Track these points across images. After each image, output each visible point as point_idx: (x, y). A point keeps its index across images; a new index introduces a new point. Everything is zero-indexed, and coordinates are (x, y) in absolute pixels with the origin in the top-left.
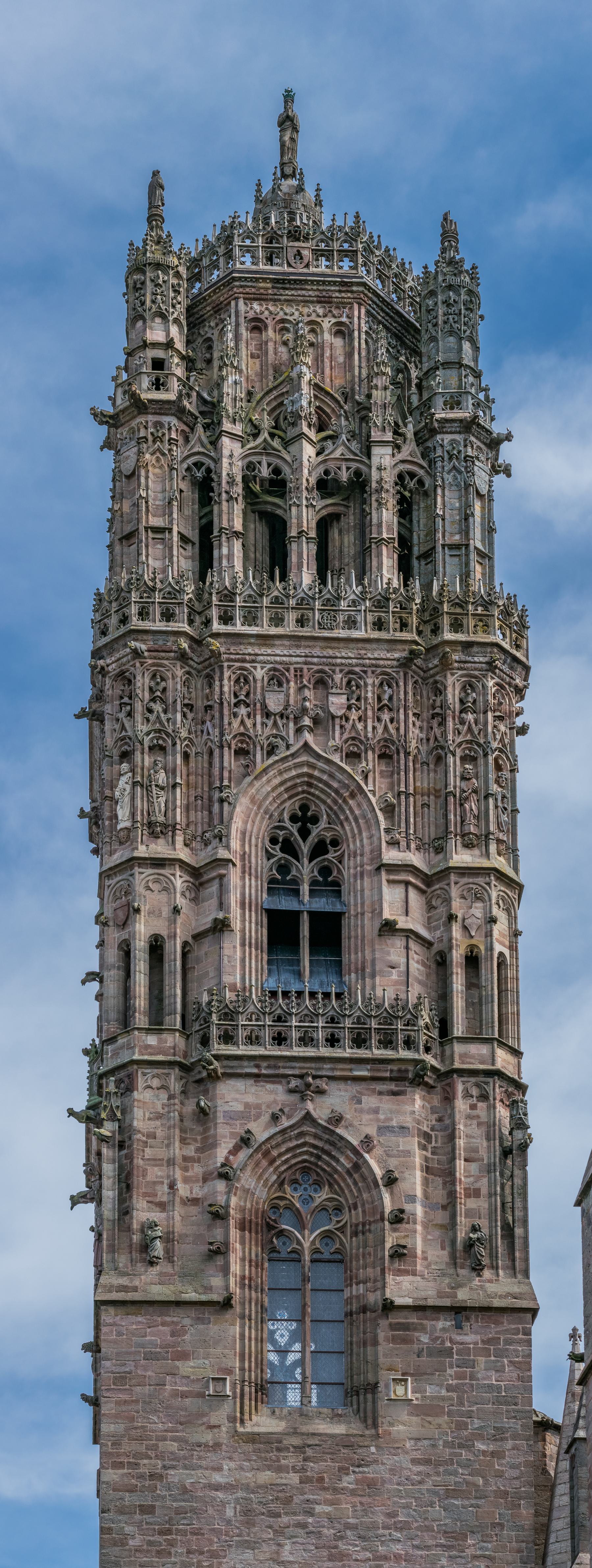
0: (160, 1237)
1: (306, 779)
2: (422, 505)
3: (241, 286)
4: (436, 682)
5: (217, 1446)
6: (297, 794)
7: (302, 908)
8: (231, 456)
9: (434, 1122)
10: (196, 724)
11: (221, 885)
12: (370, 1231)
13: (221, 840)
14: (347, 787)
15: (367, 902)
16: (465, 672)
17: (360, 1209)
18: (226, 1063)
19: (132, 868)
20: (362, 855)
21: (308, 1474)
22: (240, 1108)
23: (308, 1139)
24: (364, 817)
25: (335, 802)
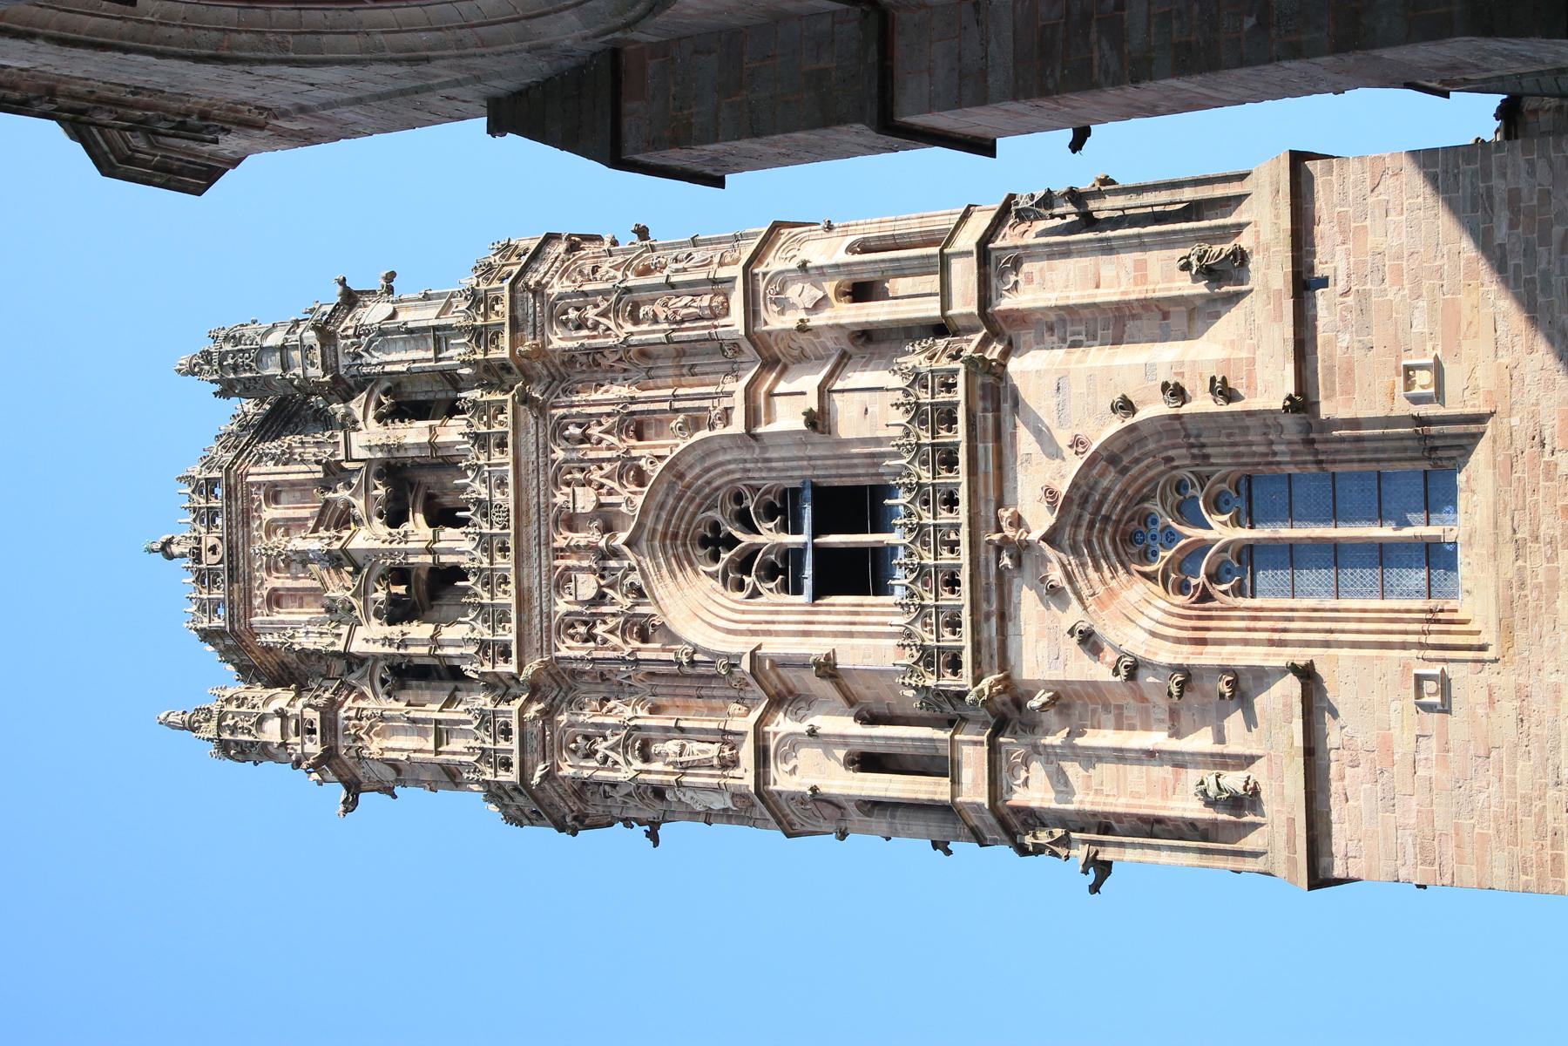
0: (1218, 777)
1: (668, 542)
2: (409, 389)
3: (239, 621)
4: (563, 363)
5: (1522, 694)
6: (687, 553)
7: (810, 546)
8: (367, 641)
9: (1055, 338)
10: (624, 692)
11: (784, 665)
12: (1198, 436)
13: (735, 665)
14: (672, 486)
15: (795, 452)
16: (546, 325)
17: (1171, 453)
18: (985, 667)
19: (770, 793)
20: (745, 461)
21: (1558, 533)
22: (1043, 643)
23: (1081, 536)
24: (703, 459)
25: (692, 500)
